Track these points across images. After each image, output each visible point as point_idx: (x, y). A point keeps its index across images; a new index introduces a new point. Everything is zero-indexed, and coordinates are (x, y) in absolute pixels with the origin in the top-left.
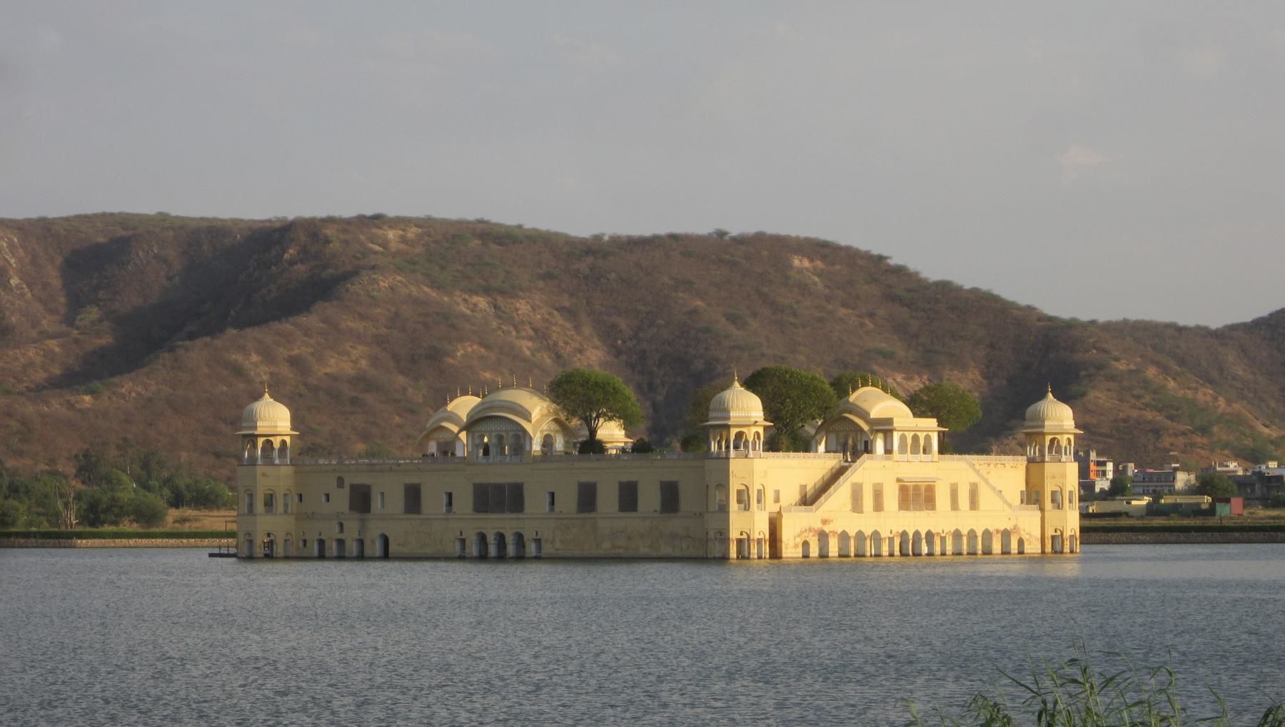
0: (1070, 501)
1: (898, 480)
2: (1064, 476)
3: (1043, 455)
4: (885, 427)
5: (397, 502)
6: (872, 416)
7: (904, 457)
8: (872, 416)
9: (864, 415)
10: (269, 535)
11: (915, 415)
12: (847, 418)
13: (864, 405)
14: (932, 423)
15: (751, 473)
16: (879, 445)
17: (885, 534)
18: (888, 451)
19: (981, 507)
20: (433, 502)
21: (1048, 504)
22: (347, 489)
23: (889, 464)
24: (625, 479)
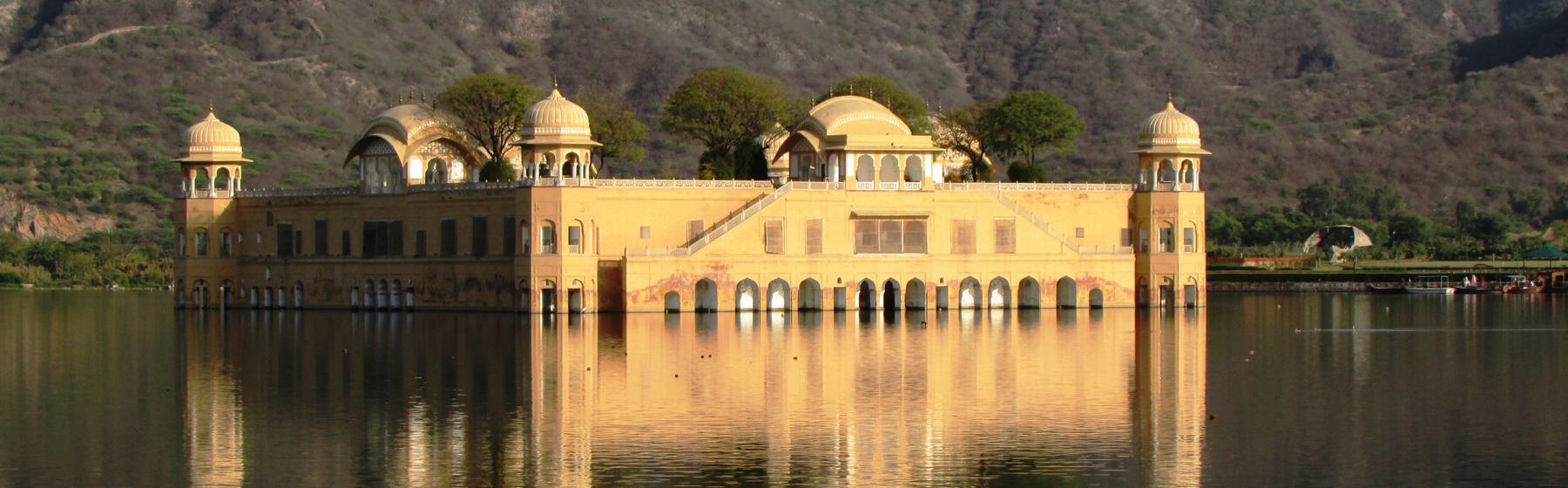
0: (1188, 241)
1: (853, 216)
2: (1176, 209)
3: (1151, 182)
4: (836, 147)
5: (309, 245)
6: (829, 133)
7: (870, 185)
8: (829, 133)
9: (818, 130)
10: (202, 282)
11: (914, 132)
12: (801, 137)
13: (822, 119)
14: (925, 142)
15: (557, 205)
16: (836, 171)
17: (827, 284)
18: (842, 178)
19: (1019, 249)
20: (335, 247)
21: (1157, 246)
22: (275, 229)
23: (840, 195)
24: (476, 215)
